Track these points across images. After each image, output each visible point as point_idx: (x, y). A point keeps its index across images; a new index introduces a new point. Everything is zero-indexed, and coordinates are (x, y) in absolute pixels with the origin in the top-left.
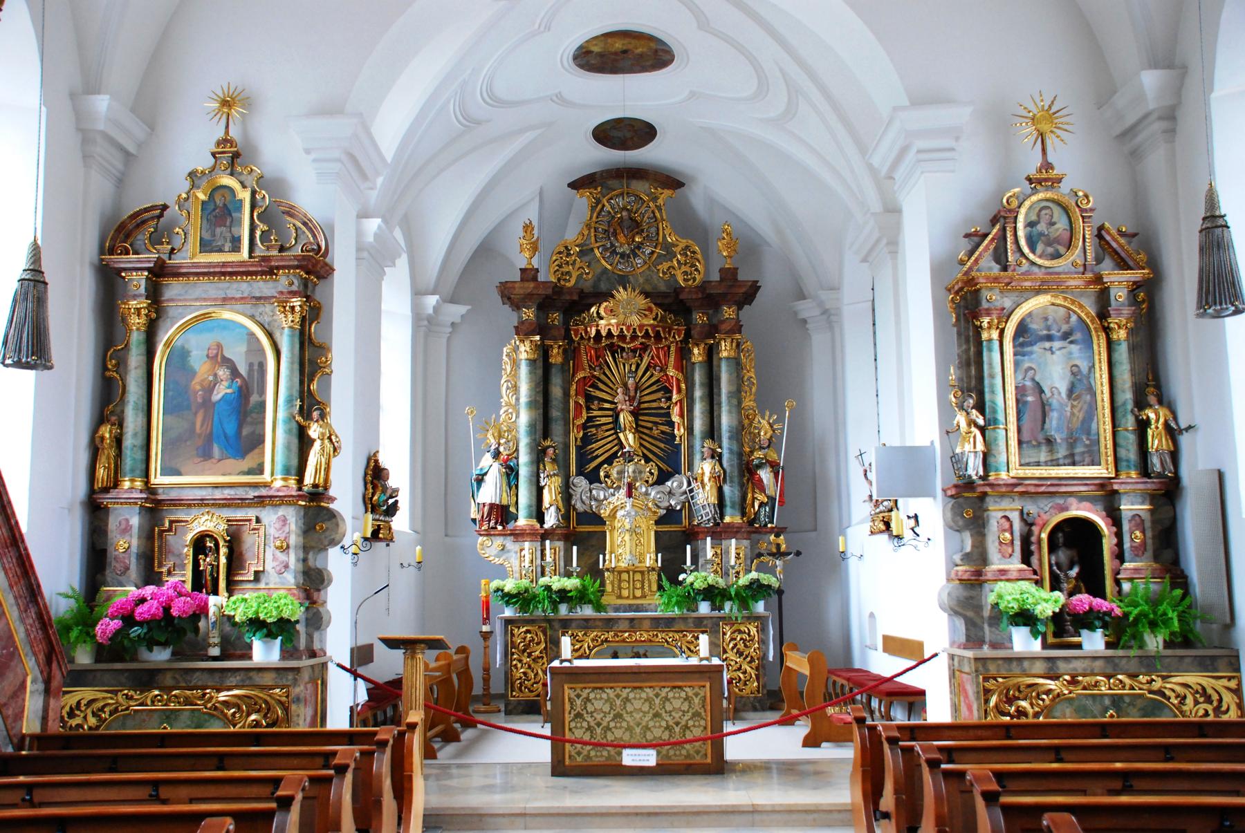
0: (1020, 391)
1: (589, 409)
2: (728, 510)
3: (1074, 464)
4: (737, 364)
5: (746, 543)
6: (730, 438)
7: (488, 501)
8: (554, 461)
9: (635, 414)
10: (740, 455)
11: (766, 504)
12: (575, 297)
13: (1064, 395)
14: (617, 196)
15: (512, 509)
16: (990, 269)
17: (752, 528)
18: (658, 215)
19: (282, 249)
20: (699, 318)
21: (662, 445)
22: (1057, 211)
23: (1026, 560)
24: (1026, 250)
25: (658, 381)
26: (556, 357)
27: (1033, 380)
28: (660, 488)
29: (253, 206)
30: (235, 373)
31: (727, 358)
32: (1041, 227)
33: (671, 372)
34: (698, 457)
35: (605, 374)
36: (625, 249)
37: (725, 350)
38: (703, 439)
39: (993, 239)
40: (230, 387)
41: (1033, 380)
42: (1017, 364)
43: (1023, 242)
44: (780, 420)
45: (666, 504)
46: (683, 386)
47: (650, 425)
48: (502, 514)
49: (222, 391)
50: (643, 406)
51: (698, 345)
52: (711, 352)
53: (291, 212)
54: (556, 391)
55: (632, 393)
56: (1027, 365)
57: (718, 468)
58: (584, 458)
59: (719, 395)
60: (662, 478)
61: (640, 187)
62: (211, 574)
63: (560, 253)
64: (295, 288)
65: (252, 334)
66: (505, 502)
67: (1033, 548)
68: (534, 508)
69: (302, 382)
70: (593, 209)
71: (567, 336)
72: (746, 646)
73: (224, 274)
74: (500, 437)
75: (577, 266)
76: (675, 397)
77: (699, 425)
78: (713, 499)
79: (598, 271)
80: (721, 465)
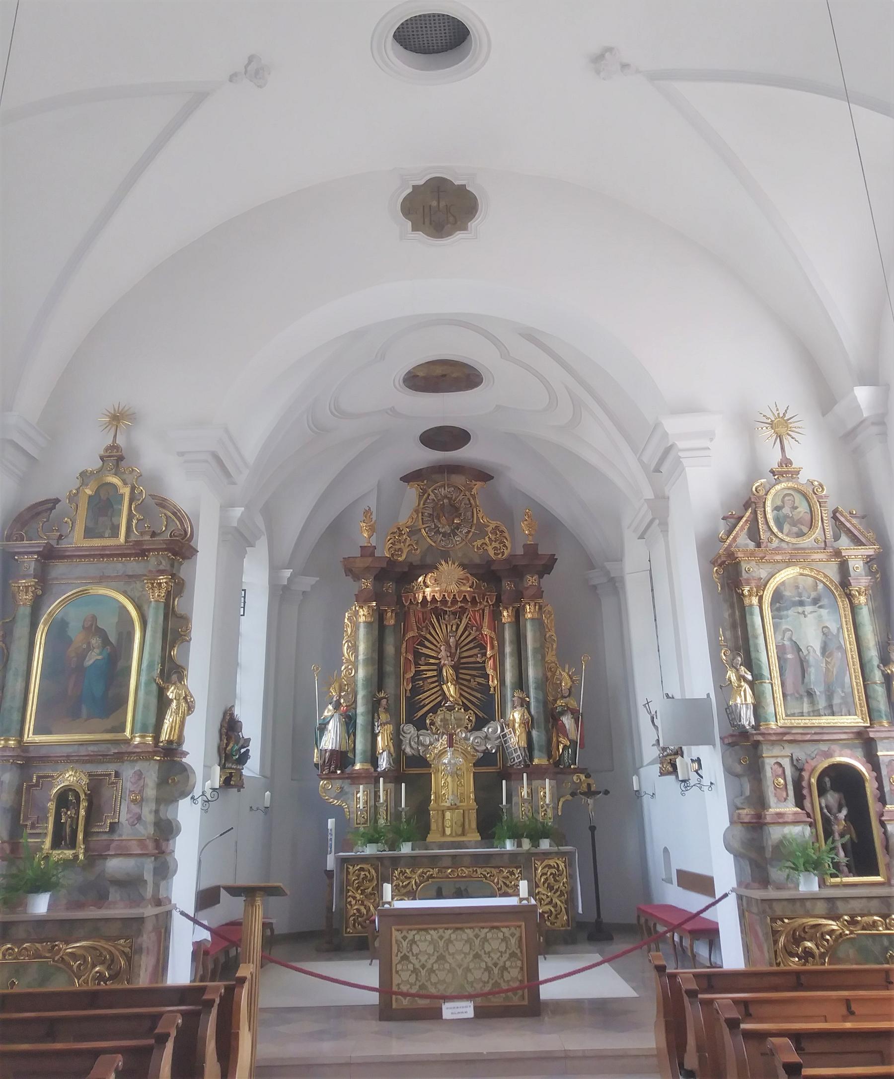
0: (781, 649)
1: (417, 664)
2: (536, 753)
3: (833, 714)
7: (330, 748)
8: (387, 710)
9: (455, 668)
10: (545, 703)
11: (569, 747)
12: (406, 570)
13: (818, 653)
14: (440, 487)
15: (350, 755)
16: (747, 545)
17: (558, 769)
18: (472, 501)
19: (154, 534)
20: (507, 585)
21: (479, 695)
22: (798, 498)
23: (799, 803)
24: (775, 530)
25: (475, 639)
27: (791, 639)
28: (478, 733)
29: (131, 501)
30: (106, 641)
31: (532, 619)
32: (786, 510)
33: (486, 631)
34: (509, 705)
35: (430, 634)
36: (447, 529)
37: (529, 612)
38: (513, 690)
39: (746, 521)
40: (100, 654)
41: (791, 639)
42: (776, 627)
43: (772, 523)
44: (578, 672)
47: (468, 677)
48: (340, 760)
49: (94, 657)
52: (518, 615)
53: (163, 503)
54: (390, 649)
55: (453, 651)
56: (784, 627)
57: (526, 716)
58: (413, 706)
60: (479, 725)
61: (459, 480)
62: (71, 826)
64: (161, 567)
65: (123, 608)
66: (343, 749)
67: (805, 792)
68: (369, 753)
69: (163, 649)
70: (420, 497)
71: (399, 602)
72: (556, 881)
73: (103, 556)
74: (341, 690)
77: (509, 677)
78: (523, 743)
80: (529, 712)
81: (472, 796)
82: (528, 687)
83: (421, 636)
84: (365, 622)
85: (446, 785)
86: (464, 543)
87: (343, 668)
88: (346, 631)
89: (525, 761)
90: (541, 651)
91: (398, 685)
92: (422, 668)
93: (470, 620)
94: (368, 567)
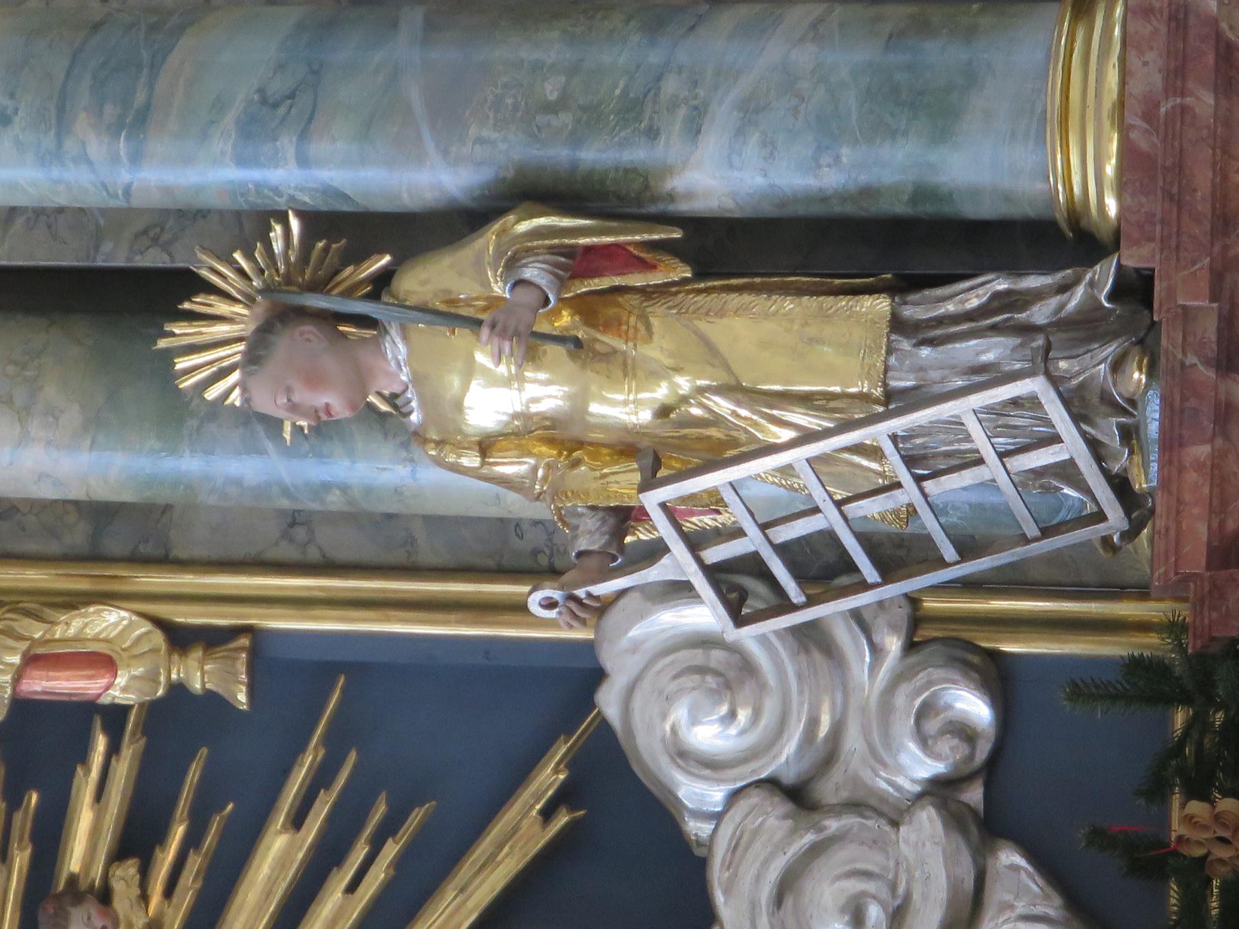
2: (980, 167)
6: (136, 122)
34: (375, 472)
38: (178, 412)
45: (927, 852)
78: (828, 338)
89: (1085, 328)
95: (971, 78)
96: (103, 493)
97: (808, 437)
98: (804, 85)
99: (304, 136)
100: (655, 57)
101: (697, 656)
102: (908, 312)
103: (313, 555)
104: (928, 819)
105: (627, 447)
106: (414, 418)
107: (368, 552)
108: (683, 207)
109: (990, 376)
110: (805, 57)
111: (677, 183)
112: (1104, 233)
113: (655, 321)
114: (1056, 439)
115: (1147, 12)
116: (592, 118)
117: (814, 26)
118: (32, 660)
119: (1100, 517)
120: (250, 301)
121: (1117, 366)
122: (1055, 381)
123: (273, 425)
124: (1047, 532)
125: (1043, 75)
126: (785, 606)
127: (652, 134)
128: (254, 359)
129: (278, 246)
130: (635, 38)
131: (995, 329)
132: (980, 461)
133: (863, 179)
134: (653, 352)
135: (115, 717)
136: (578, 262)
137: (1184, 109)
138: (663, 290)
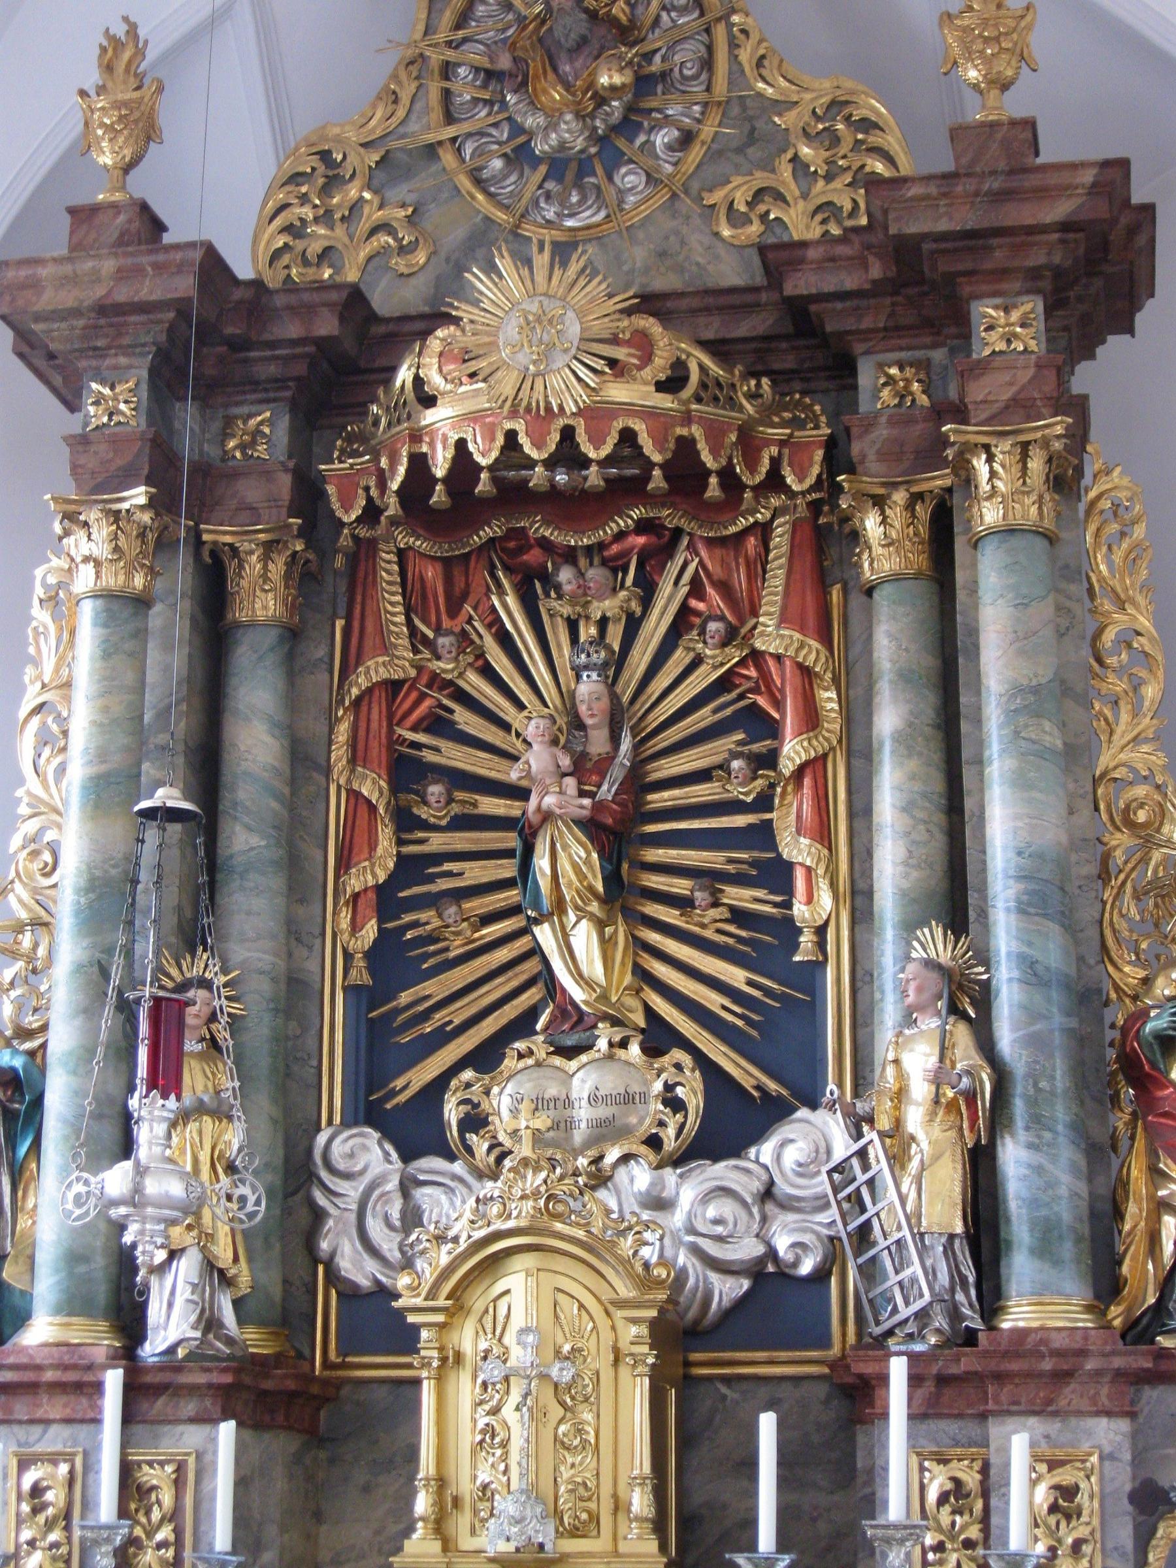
2: (1021, 1268)
4: (1057, 551)
5: (1108, 1433)
6: (1022, 909)
9: (616, 836)
10: (1087, 998)
12: (327, 326)
20: (885, 384)
21: (736, 976)
25: (723, 684)
26: (261, 599)
28: (721, 1171)
31: (1008, 531)
33: (772, 635)
34: (889, 1013)
35: (488, 673)
36: (568, 134)
38: (909, 928)
45: (747, 1249)
46: (828, 699)
47: (680, 886)
50: (660, 799)
51: (879, 502)
55: (598, 743)
58: (379, 1046)
59: (978, 721)
60: (730, 1125)
63: (296, 178)
71: (309, 497)
75: (364, 226)
76: (793, 751)
77: (893, 867)
78: (944, 1210)
79: (460, 233)
81: (640, 1502)
82: (983, 914)
83: (435, 681)
84: (106, 596)
85: (490, 1438)
86: (663, 196)
87: (16, 841)
88: (36, 662)
89: (955, 1315)
90: (1069, 698)
91: (297, 934)
92: (437, 842)
93: (696, 590)
94: (103, 309)
95: (1057, 1262)
96: (876, 896)
97: (903, 1200)
98: (1050, 1192)
99: (1020, 980)
100: (1060, 1128)
101: (822, 1150)
102: (957, 1243)
103: (859, 984)
104: (760, 1250)
105: (898, 1123)
106: (907, 1032)
107: (861, 1008)
108: (999, 1142)
109: (931, 1274)
110: (1063, 1191)
111: (1008, 1140)
112: (995, 1323)
113: (949, 1133)
114: (907, 1303)
115: (1086, 1338)
116: (1032, 1102)
117: (1076, 1194)
118: (809, 870)
119: (878, 1323)
120: (953, 959)
121: (938, 1331)
122: (931, 1303)
123: (903, 970)
124: (870, 1301)
125: (1060, 1294)
126: (836, 1191)
127: (1027, 1128)
128: (930, 964)
129: (976, 970)
130: (1067, 1118)
131: (952, 1277)
132: (897, 1272)
133: (1014, 1219)
134: (936, 1131)
135: (788, 905)
136: (971, 1097)
137: (1044, 1357)
138: (962, 1136)
